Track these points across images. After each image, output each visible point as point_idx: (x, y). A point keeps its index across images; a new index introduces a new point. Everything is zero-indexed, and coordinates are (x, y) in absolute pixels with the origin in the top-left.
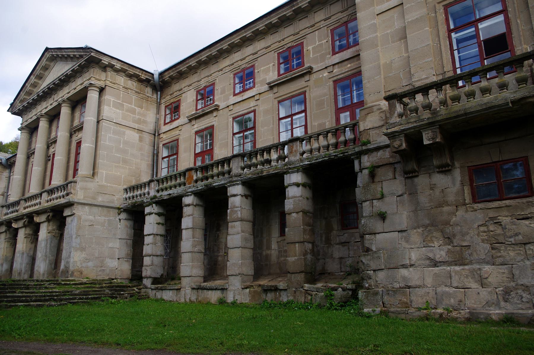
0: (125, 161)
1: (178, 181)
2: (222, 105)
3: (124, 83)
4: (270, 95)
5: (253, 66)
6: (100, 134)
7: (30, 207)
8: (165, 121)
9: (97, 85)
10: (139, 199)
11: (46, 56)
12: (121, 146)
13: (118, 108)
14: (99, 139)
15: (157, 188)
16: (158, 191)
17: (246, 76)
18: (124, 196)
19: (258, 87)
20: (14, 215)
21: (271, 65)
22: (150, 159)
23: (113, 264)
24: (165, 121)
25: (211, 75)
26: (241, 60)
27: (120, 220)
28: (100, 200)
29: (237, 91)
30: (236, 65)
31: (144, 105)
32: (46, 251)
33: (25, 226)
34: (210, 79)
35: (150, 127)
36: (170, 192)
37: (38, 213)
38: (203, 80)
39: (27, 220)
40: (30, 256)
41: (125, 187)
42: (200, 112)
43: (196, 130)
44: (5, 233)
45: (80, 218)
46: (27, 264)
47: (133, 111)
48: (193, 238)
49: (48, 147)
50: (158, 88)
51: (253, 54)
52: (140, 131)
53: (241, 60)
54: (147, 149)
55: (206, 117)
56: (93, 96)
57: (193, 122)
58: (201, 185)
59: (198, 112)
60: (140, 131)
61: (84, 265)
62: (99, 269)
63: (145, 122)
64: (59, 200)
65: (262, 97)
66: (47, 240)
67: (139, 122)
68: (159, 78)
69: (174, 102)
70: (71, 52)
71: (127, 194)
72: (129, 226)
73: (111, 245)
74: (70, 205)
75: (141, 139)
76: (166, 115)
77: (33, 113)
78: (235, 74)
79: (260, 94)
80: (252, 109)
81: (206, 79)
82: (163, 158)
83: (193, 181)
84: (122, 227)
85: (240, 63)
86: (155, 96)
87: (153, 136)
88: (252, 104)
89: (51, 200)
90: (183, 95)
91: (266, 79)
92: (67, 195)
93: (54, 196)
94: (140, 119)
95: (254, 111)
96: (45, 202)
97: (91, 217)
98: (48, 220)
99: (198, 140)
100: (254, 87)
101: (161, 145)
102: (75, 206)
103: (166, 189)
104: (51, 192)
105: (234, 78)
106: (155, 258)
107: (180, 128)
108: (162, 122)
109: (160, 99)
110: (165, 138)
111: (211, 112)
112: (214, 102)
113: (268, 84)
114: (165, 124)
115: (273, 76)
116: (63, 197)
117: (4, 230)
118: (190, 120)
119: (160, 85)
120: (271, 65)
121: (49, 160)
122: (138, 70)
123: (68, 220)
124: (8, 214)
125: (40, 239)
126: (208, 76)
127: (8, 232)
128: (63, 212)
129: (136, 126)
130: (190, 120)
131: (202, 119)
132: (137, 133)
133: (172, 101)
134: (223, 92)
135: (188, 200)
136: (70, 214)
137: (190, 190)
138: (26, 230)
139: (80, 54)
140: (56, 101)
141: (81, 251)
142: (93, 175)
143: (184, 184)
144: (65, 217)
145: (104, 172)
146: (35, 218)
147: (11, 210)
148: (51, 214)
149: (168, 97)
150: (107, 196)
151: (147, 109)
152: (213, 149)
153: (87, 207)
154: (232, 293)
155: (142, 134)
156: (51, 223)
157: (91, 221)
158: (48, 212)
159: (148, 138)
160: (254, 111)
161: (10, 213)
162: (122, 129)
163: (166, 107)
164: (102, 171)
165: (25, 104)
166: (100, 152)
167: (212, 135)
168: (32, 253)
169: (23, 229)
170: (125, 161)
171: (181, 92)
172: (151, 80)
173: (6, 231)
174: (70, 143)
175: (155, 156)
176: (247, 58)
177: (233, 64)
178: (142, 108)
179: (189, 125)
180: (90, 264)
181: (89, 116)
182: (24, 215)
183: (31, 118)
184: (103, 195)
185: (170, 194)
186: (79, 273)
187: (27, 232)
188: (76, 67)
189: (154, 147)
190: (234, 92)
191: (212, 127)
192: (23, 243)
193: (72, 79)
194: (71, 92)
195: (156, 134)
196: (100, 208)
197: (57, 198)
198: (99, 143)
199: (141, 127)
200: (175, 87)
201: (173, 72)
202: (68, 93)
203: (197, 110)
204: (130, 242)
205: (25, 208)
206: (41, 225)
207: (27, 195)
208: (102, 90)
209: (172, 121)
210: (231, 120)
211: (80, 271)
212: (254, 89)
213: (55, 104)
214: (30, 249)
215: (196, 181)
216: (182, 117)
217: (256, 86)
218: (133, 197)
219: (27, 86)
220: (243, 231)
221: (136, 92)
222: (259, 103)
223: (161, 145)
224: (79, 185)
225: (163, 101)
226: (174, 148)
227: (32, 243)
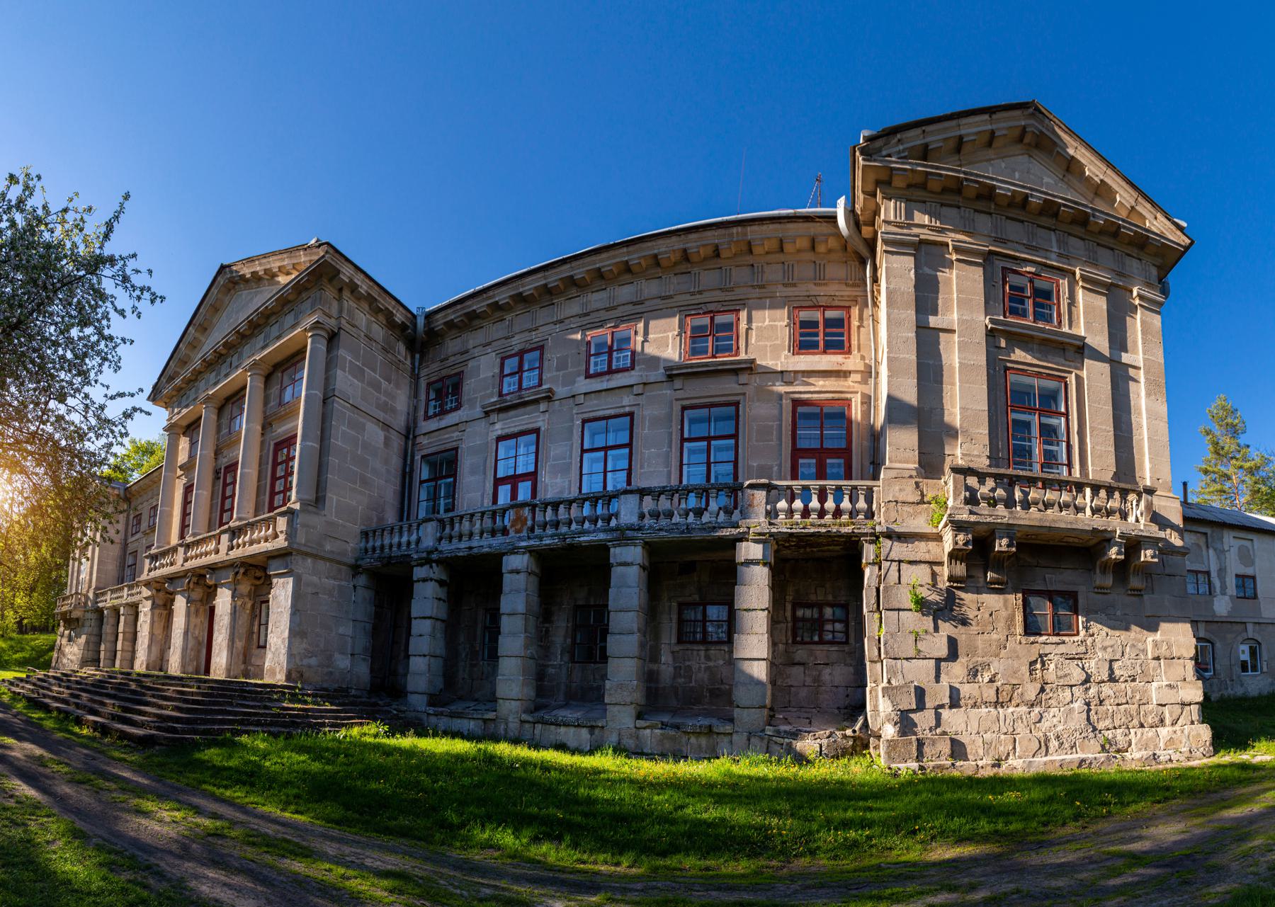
2: (561, 391)
22: (398, 481)
24: (426, 412)
25: (536, 329)
34: (535, 337)
35: (400, 422)
38: (517, 337)
43: (499, 432)
54: (396, 461)
55: (521, 410)
57: (494, 417)
63: (393, 410)
69: (450, 376)
75: (387, 441)
76: (428, 400)
79: (645, 384)
80: (627, 409)
81: (526, 336)
82: (422, 482)
88: (627, 401)
90: (470, 364)
94: (386, 404)
95: (631, 415)
100: (633, 368)
101: (418, 458)
107: (461, 427)
108: (421, 413)
110: (427, 444)
111: (536, 401)
112: (540, 385)
114: (427, 418)
126: (530, 331)
129: (381, 415)
130: (487, 414)
131: (512, 413)
133: (444, 373)
134: (562, 365)
137: (523, 544)
149: (435, 366)
151: (397, 386)
159: (397, 442)
160: (631, 415)
163: (429, 384)
171: (465, 357)
175: (406, 475)
179: (483, 423)
185: (471, 548)
195: (410, 434)
200: (452, 345)
203: (501, 395)
209: (443, 412)
212: (633, 373)
216: (466, 406)
222: (640, 400)
225: (424, 372)
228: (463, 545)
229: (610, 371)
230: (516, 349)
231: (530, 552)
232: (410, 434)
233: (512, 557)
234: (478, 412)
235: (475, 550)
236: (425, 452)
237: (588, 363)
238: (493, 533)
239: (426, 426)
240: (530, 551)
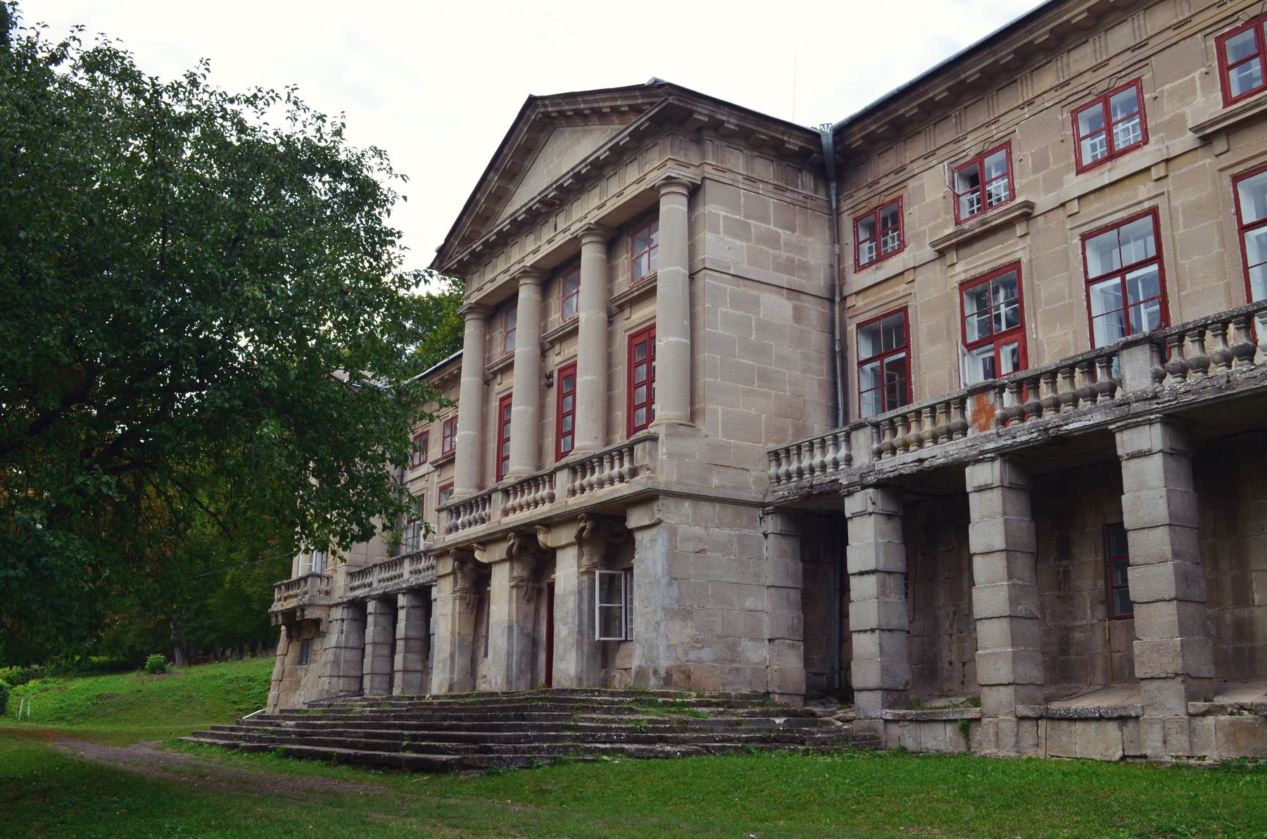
0: (765, 377)
1: (942, 422)
2: (1043, 201)
3: (747, 166)
4: (1206, 161)
5: (1137, 82)
6: (699, 308)
7: (521, 508)
8: (857, 260)
9: (685, 180)
10: (819, 478)
11: (529, 117)
12: (753, 338)
13: (736, 236)
14: (700, 320)
15: (875, 446)
16: (879, 453)
18: (773, 471)
19: (1157, 142)
20: (479, 530)
21: (1197, 74)
22: (825, 367)
23: (756, 653)
24: (857, 260)
25: (996, 120)
26: (1095, 69)
27: (766, 536)
28: (716, 483)
29: (1087, 160)
30: (1075, 86)
31: (799, 221)
32: (581, 621)
33: (510, 557)
34: (996, 132)
35: (817, 282)
36: (924, 453)
37: (549, 524)
38: (970, 138)
39: (517, 541)
40: (528, 635)
41: (772, 446)
42: (972, 225)
43: (963, 277)
44: (451, 577)
45: (673, 532)
46: (522, 654)
47: (773, 241)
48: (1010, 578)
49: (544, 353)
51: (1133, 49)
52: (794, 292)
53: (1095, 69)
54: (817, 339)
55: (991, 240)
56: (672, 208)
57: (952, 257)
58: (1023, 432)
60: (794, 292)
61: (693, 655)
62: (728, 666)
63: (804, 267)
64: (607, 488)
65: (1178, 170)
66: (580, 592)
67: (789, 267)
68: (835, 143)
69: (883, 206)
70: (604, 100)
71: (779, 465)
72: (789, 551)
73: (749, 603)
74: (647, 498)
75: (798, 315)
76: (858, 244)
77: (495, 267)
78: (1075, 113)
79: (1167, 161)
80: (1146, 205)
81: (982, 134)
83: (993, 422)
84: (771, 554)
85: (1089, 78)
86: (821, 195)
87: (827, 304)
88: (1143, 191)
89: (583, 490)
90: (911, 184)
92: (634, 473)
94: (790, 261)
95: (1154, 212)
96: (565, 495)
97: (698, 530)
98: (580, 541)
99: (971, 308)
100: (1146, 141)
101: (852, 328)
102: (660, 502)
103: (906, 446)
105: (1075, 122)
106: (886, 635)
108: (849, 262)
109: (838, 201)
110: (864, 308)
111: (1009, 225)
112: (1012, 196)
113: (1195, 130)
114: (859, 268)
115: (1207, 105)
116: (621, 478)
117: (449, 570)
118: (942, 253)
119: (834, 165)
120: (1197, 74)
121: (550, 385)
122: (781, 128)
123: (641, 538)
124: (457, 529)
125: (558, 590)
126: (988, 125)
127: (459, 575)
128: (625, 519)
129: (783, 279)
130: (942, 253)
131: (978, 246)
132: (788, 298)
133: (875, 202)
134: (1041, 163)
135: (976, 476)
136: (646, 522)
138: (512, 569)
139: (631, 102)
140: (565, 231)
141: (684, 619)
142: (693, 416)
143: (964, 429)
144: (631, 532)
145: (720, 409)
146: (541, 538)
147: (463, 519)
148: (588, 525)
149: (862, 194)
150: (731, 472)
151: (807, 231)
152: (1022, 328)
153: (687, 504)
154: (1157, 729)
155: (799, 299)
156: (586, 550)
157: (700, 540)
158: (582, 519)
159: (815, 311)
160: (1154, 212)
161: (464, 526)
162: (752, 291)
164: (716, 410)
165: (477, 246)
166: (703, 356)
168: (530, 626)
169: (507, 566)
170: (765, 377)
172: (812, 152)
173: (453, 573)
174: (609, 337)
175: (837, 357)
176: (1113, 63)
177: (1066, 83)
178: (794, 231)
179: (938, 266)
180: (706, 654)
181: (663, 259)
182: (510, 530)
183: (493, 280)
184: (722, 469)
185: (921, 461)
186: (683, 677)
187: (515, 574)
188: (623, 139)
189: (833, 333)
190: (1078, 161)
191: (1016, 265)
192: (510, 601)
193: (609, 172)
194: (609, 204)
195: (835, 296)
196: (718, 506)
197: (601, 484)
198: (700, 334)
199: (797, 281)
200: (885, 164)
201: (875, 122)
202: (599, 208)
203: (958, 222)
204: (795, 596)
205: (506, 513)
206: (560, 555)
207: (509, 480)
208: (694, 193)
209: (881, 258)
211: (684, 672)
212: (1146, 148)
213: (561, 239)
214: (526, 616)
215: (1004, 421)
217: (1152, 139)
218: (800, 473)
219: (479, 201)
220: (1176, 555)
221: (776, 187)
223: (852, 328)
224: (662, 449)
225: (845, 205)
227: (528, 601)
228: (910, 457)
229: (1113, 155)
230: (972, 154)
231: (1002, 455)
232: (835, 296)
233: (979, 467)
234: (928, 253)
235: (926, 464)
236: (862, 319)
237: (1078, 151)
238: (949, 434)
239: (857, 281)
240: (1004, 454)
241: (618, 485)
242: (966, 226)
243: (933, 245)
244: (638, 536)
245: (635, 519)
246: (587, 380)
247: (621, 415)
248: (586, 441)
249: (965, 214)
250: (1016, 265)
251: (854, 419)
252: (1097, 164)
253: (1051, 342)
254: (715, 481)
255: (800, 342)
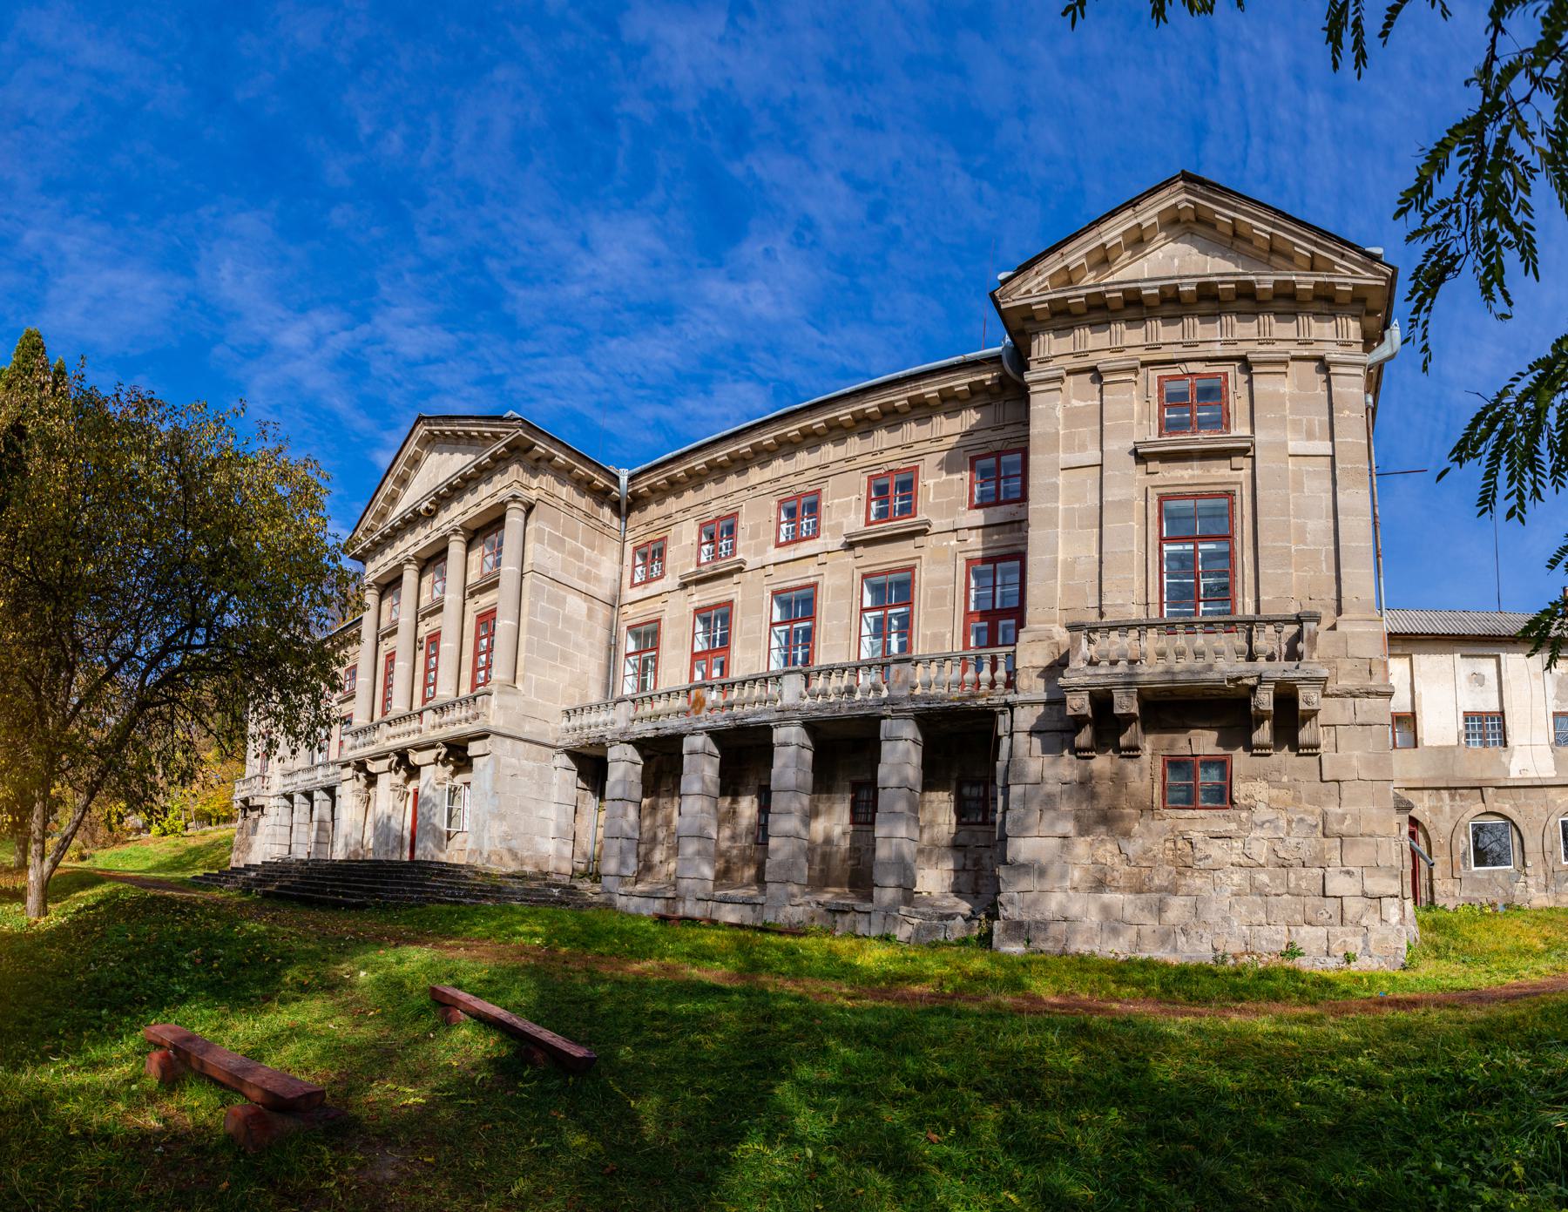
2: (752, 562)
4: (848, 558)
17: (802, 510)
22: (603, 655)
25: (731, 494)
28: (527, 730)
34: (730, 503)
35: (604, 592)
41: (565, 707)
42: (707, 570)
45: (497, 761)
50: (623, 508)
54: (601, 634)
57: (692, 589)
59: (703, 568)
63: (598, 579)
64: (458, 726)
74: (483, 736)
76: (634, 567)
80: (812, 580)
82: (627, 655)
91: (840, 525)
92: (476, 717)
93: (446, 718)
99: (700, 627)
104: (441, 709)
108: (626, 581)
110: (634, 615)
111: (729, 574)
114: (633, 585)
116: (467, 720)
118: (684, 586)
126: (726, 496)
133: (650, 537)
134: (754, 535)
148: (444, 751)
163: (635, 549)
167: (727, 619)
171: (669, 521)
175: (612, 647)
191: (730, 603)
203: (699, 565)
210: (769, 594)
213: (435, 536)
216: (669, 575)
223: (624, 629)
226: (648, 635)
230: (713, 517)
232: (615, 603)
239: (631, 594)
241: (465, 725)
242: (703, 568)
243: (681, 577)
244: (475, 760)
245: (474, 748)
246: (448, 646)
247: (467, 674)
248: (445, 692)
249: (704, 559)
250: (730, 603)
251: (618, 695)
252: (788, 543)
253: (744, 661)
254: (527, 728)
255: (590, 634)
